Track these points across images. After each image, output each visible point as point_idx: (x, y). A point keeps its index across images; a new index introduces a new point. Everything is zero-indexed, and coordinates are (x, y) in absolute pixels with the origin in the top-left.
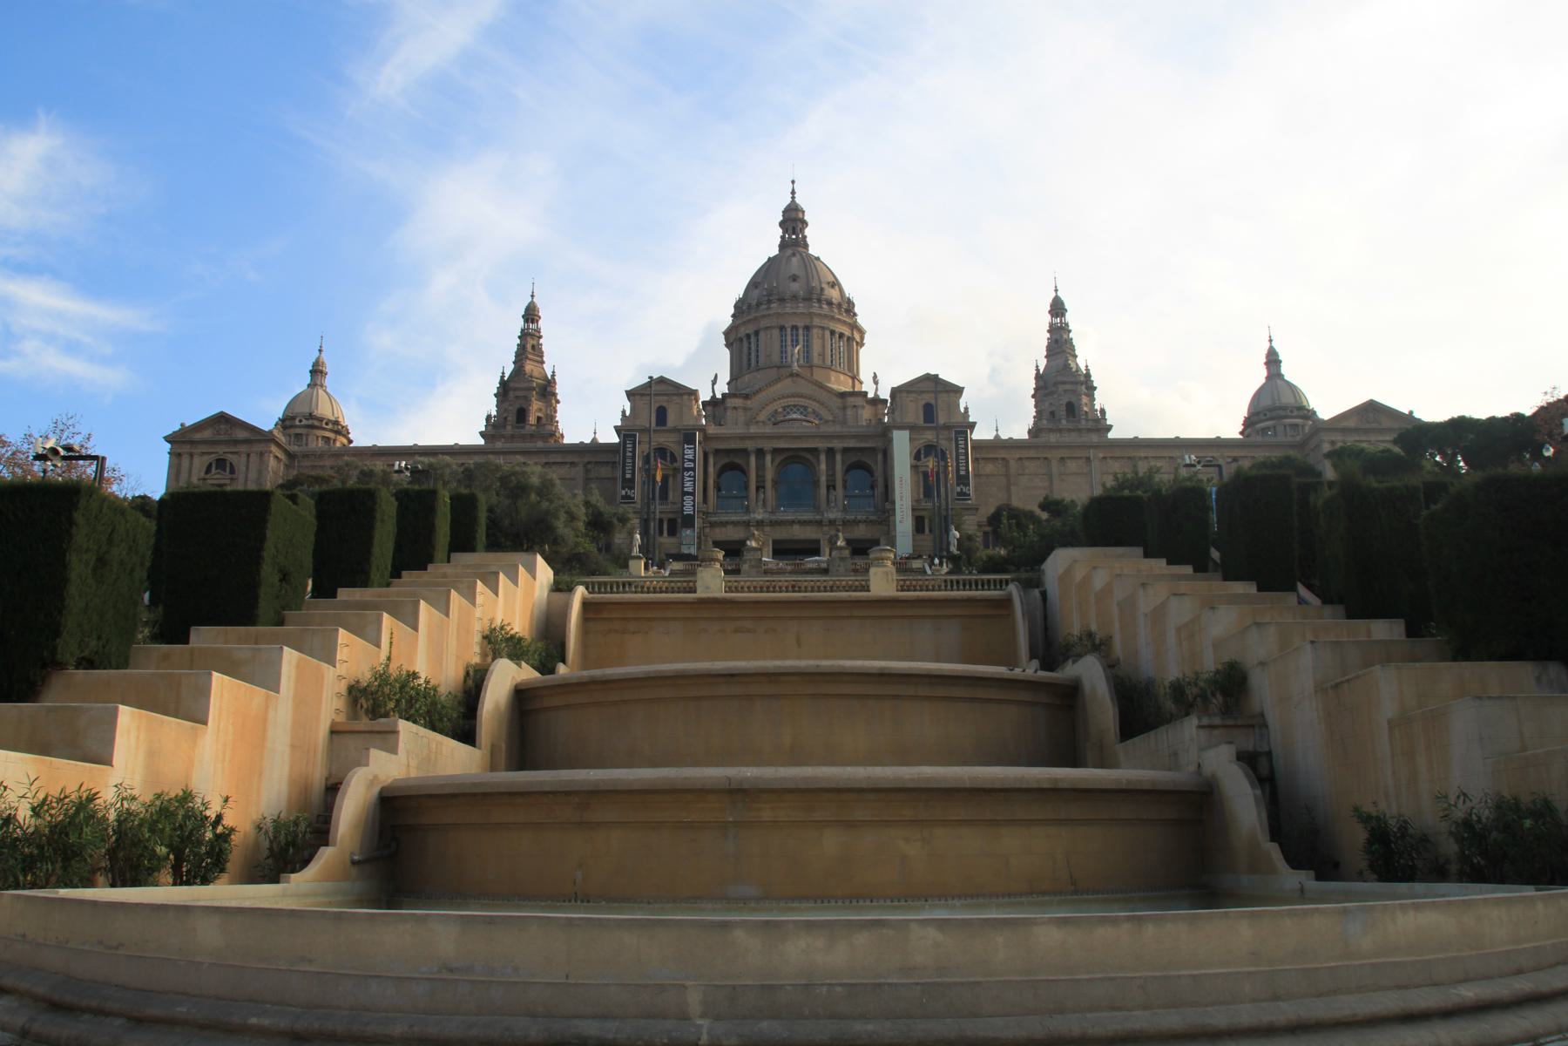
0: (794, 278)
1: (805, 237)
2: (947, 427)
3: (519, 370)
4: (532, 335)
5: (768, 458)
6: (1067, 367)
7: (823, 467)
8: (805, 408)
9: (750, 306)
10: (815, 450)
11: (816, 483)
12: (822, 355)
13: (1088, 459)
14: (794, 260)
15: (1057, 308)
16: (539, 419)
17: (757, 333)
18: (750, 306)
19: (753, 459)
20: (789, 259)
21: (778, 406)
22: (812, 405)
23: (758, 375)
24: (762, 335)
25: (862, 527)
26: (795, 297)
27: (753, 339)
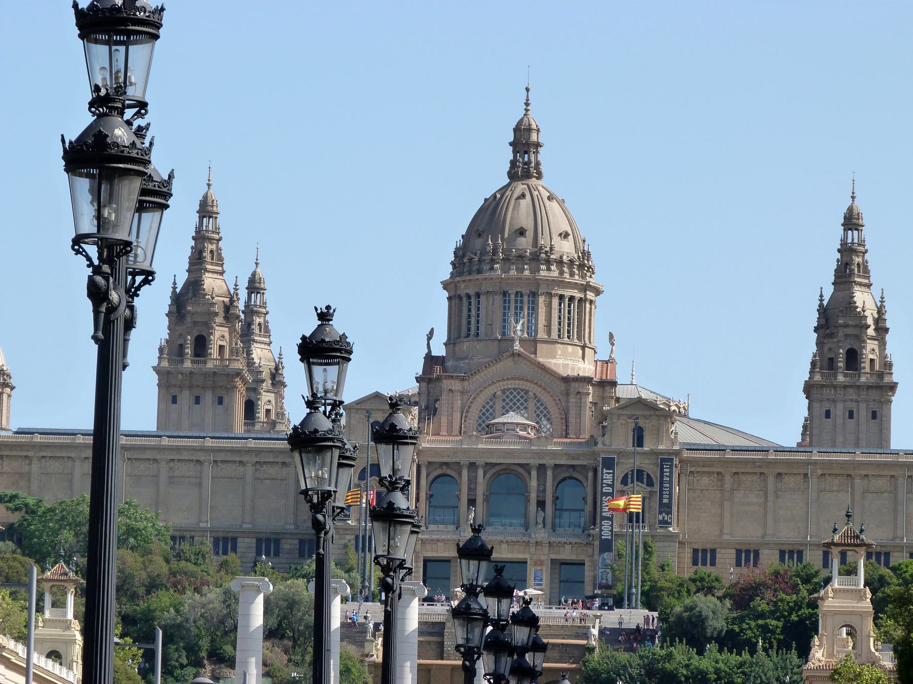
0: (522, 232)
1: (538, 164)
2: (654, 453)
3: (194, 285)
4: (210, 240)
5: (480, 472)
6: (850, 305)
7: (534, 483)
8: (527, 392)
9: (471, 260)
10: (528, 464)
11: (528, 500)
12: (548, 326)
13: (806, 475)
14: (525, 203)
15: (851, 222)
16: (221, 348)
17: (478, 295)
18: (471, 260)
19: (465, 473)
20: (517, 206)
21: (497, 389)
22: (533, 389)
23: (479, 346)
24: (483, 299)
25: (568, 547)
26: (521, 257)
27: (473, 300)
